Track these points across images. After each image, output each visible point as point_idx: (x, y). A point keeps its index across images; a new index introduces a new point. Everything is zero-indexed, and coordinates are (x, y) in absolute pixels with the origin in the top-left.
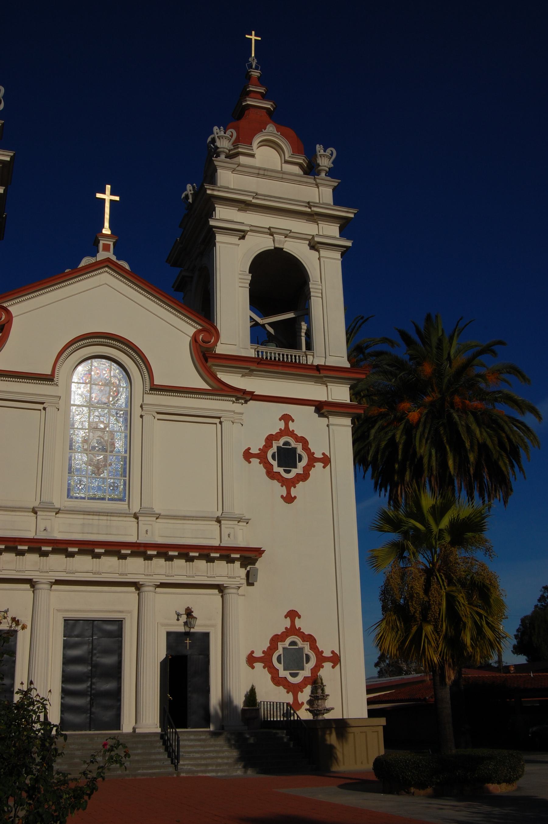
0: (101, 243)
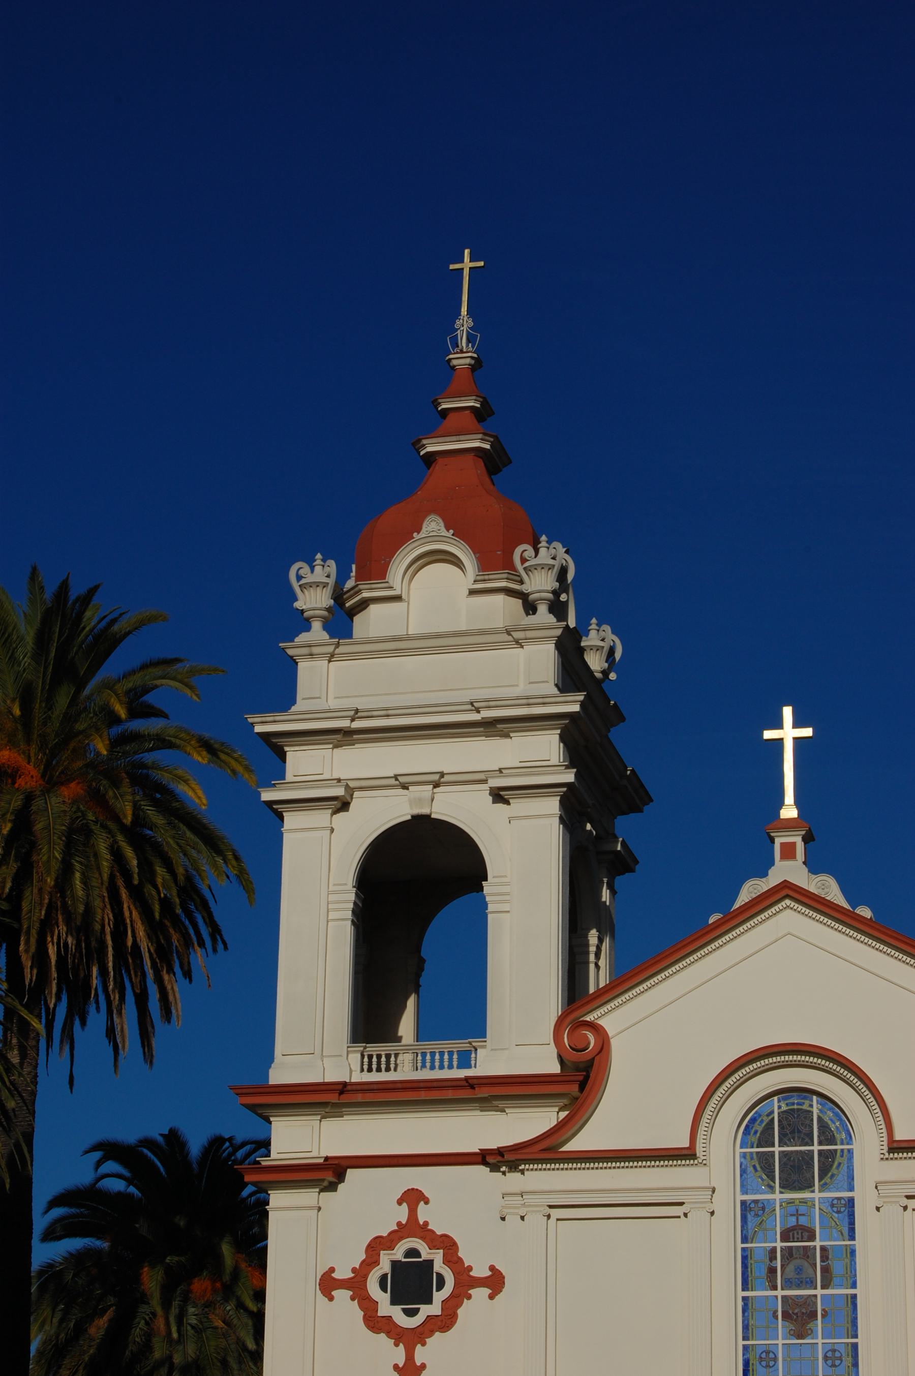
0: (778, 841)
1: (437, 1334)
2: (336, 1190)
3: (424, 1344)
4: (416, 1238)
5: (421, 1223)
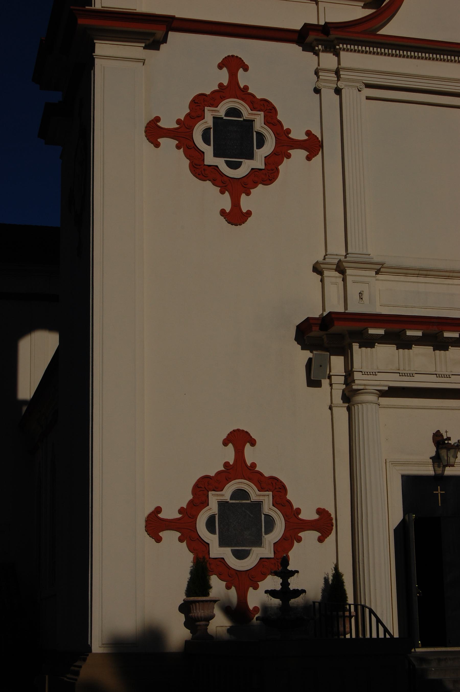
1: (260, 186)
2: (158, 49)
3: (248, 194)
4: (238, 99)
5: (242, 87)
